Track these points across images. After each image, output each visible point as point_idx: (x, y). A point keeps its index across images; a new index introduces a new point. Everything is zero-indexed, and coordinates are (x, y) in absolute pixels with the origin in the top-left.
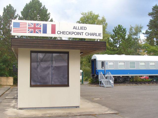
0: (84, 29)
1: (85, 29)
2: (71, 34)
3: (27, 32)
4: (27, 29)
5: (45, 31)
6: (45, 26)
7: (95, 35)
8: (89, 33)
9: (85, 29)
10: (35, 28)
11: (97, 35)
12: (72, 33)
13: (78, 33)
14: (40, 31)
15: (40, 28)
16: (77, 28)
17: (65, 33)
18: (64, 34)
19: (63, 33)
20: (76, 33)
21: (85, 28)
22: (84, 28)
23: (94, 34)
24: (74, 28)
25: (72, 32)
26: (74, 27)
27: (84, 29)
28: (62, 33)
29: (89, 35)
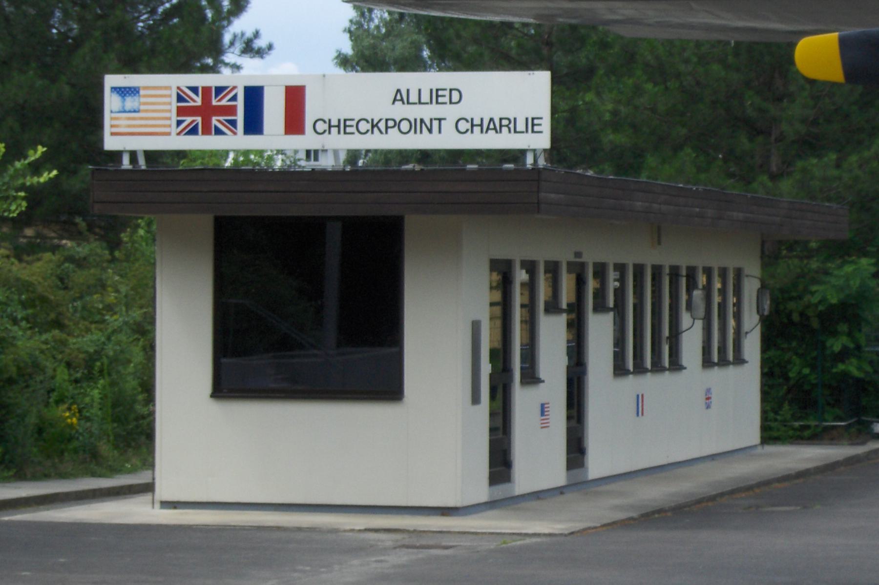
0: (451, 103)
2: (383, 130)
3: (174, 130)
4: (175, 118)
5: (254, 125)
7: (505, 129)
9: (455, 96)
10: (206, 111)
11: (521, 126)
12: (387, 128)
13: (417, 125)
14: (233, 123)
15: (232, 110)
16: (414, 98)
17: (354, 130)
18: (345, 133)
19: (343, 126)
20: (405, 126)
21: (455, 96)
22: (447, 93)
23: (501, 126)
25: (387, 120)
26: (398, 91)
27: (447, 99)
28: (334, 130)
29: (477, 129)
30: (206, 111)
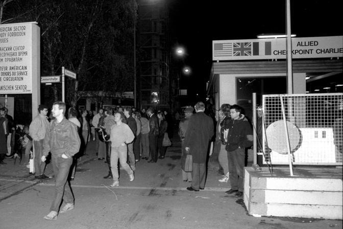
1: (316, 43)
3: (233, 55)
5: (256, 52)
6: (256, 46)
8: (323, 50)
9: (316, 43)
11: (336, 51)
12: (296, 52)
13: (305, 52)
14: (250, 52)
15: (250, 49)
20: (301, 52)
21: (316, 44)
24: (299, 44)
26: (299, 42)
28: (280, 54)
29: (323, 52)
30: (242, 49)
